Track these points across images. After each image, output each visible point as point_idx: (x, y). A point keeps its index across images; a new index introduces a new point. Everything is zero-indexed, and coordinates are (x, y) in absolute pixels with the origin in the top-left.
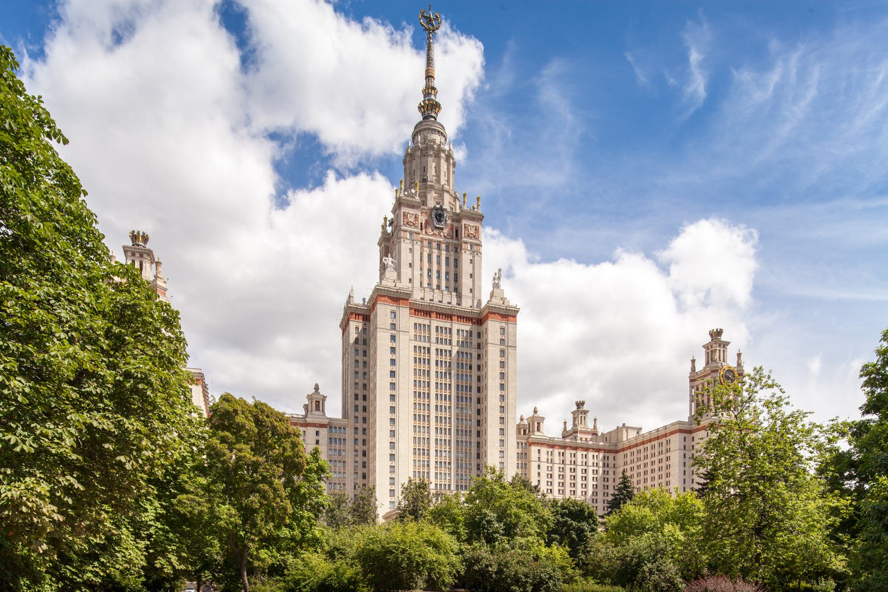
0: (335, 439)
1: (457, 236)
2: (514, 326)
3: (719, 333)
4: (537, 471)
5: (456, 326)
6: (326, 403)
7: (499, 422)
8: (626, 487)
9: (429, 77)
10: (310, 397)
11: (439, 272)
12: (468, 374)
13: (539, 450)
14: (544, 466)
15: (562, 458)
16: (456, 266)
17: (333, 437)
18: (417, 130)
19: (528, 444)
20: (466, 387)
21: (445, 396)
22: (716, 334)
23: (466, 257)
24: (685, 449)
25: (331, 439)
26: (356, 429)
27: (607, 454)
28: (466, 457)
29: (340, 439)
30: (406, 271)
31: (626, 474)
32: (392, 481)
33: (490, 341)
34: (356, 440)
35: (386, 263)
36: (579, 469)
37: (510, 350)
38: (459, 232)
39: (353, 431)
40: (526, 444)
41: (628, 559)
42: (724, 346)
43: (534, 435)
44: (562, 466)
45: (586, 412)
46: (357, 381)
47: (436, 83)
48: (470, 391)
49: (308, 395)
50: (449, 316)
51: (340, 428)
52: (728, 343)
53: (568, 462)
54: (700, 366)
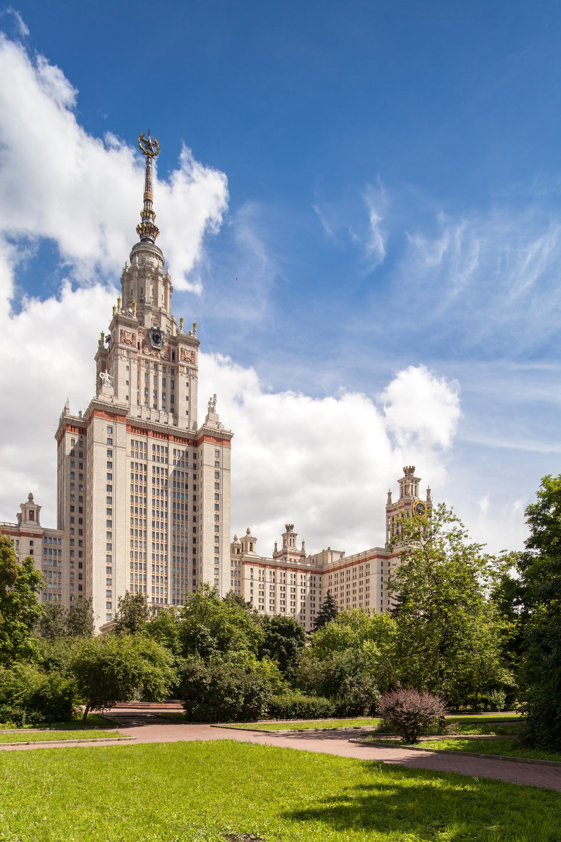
0: (50, 550)
1: (173, 358)
2: (227, 450)
3: (412, 470)
4: (250, 588)
5: (173, 446)
6: (41, 513)
7: (214, 540)
8: (331, 606)
9: (147, 200)
10: (23, 506)
11: (156, 392)
12: (185, 493)
13: (252, 569)
14: (256, 584)
15: (273, 577)
16: (173, 388)
17: (48, 547)
18: (136, 251)
19: (241, 563)
20: (183, 505)
21: (162, 513)
22: (409, 471)
23: (182, 380)
24: (382, 573)
25: (45, 549)
26: (72, 540)
27: (314, 575)
28: (182, 573)
29: (55, 550)
30: (123, 388)
31: (330, 594)
32: (109, 594)
33: (205, 462)
34: (72, 552)
35: (103, 378)
36: (289, 588)
37: (225, 473)
38: (176, 355)
39: (69, 542)
40: (239, 562)
41: (332, 672)
42: (416, 482)
43: (247, 554)
44: (273, 584)
45: (295, 535)
46: (73, 492)
47: (154, 207)
48: (187, 509)
49: (22, 504)
50: (165, 435)
51: (55, 539)
52: (420, 479)
53: (278, 581)
54: (396, 499)
